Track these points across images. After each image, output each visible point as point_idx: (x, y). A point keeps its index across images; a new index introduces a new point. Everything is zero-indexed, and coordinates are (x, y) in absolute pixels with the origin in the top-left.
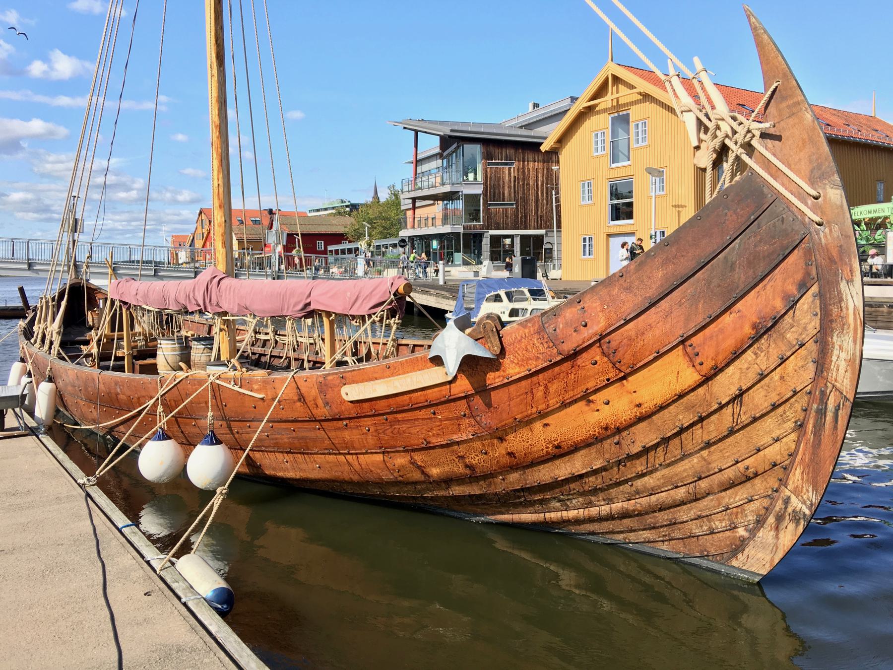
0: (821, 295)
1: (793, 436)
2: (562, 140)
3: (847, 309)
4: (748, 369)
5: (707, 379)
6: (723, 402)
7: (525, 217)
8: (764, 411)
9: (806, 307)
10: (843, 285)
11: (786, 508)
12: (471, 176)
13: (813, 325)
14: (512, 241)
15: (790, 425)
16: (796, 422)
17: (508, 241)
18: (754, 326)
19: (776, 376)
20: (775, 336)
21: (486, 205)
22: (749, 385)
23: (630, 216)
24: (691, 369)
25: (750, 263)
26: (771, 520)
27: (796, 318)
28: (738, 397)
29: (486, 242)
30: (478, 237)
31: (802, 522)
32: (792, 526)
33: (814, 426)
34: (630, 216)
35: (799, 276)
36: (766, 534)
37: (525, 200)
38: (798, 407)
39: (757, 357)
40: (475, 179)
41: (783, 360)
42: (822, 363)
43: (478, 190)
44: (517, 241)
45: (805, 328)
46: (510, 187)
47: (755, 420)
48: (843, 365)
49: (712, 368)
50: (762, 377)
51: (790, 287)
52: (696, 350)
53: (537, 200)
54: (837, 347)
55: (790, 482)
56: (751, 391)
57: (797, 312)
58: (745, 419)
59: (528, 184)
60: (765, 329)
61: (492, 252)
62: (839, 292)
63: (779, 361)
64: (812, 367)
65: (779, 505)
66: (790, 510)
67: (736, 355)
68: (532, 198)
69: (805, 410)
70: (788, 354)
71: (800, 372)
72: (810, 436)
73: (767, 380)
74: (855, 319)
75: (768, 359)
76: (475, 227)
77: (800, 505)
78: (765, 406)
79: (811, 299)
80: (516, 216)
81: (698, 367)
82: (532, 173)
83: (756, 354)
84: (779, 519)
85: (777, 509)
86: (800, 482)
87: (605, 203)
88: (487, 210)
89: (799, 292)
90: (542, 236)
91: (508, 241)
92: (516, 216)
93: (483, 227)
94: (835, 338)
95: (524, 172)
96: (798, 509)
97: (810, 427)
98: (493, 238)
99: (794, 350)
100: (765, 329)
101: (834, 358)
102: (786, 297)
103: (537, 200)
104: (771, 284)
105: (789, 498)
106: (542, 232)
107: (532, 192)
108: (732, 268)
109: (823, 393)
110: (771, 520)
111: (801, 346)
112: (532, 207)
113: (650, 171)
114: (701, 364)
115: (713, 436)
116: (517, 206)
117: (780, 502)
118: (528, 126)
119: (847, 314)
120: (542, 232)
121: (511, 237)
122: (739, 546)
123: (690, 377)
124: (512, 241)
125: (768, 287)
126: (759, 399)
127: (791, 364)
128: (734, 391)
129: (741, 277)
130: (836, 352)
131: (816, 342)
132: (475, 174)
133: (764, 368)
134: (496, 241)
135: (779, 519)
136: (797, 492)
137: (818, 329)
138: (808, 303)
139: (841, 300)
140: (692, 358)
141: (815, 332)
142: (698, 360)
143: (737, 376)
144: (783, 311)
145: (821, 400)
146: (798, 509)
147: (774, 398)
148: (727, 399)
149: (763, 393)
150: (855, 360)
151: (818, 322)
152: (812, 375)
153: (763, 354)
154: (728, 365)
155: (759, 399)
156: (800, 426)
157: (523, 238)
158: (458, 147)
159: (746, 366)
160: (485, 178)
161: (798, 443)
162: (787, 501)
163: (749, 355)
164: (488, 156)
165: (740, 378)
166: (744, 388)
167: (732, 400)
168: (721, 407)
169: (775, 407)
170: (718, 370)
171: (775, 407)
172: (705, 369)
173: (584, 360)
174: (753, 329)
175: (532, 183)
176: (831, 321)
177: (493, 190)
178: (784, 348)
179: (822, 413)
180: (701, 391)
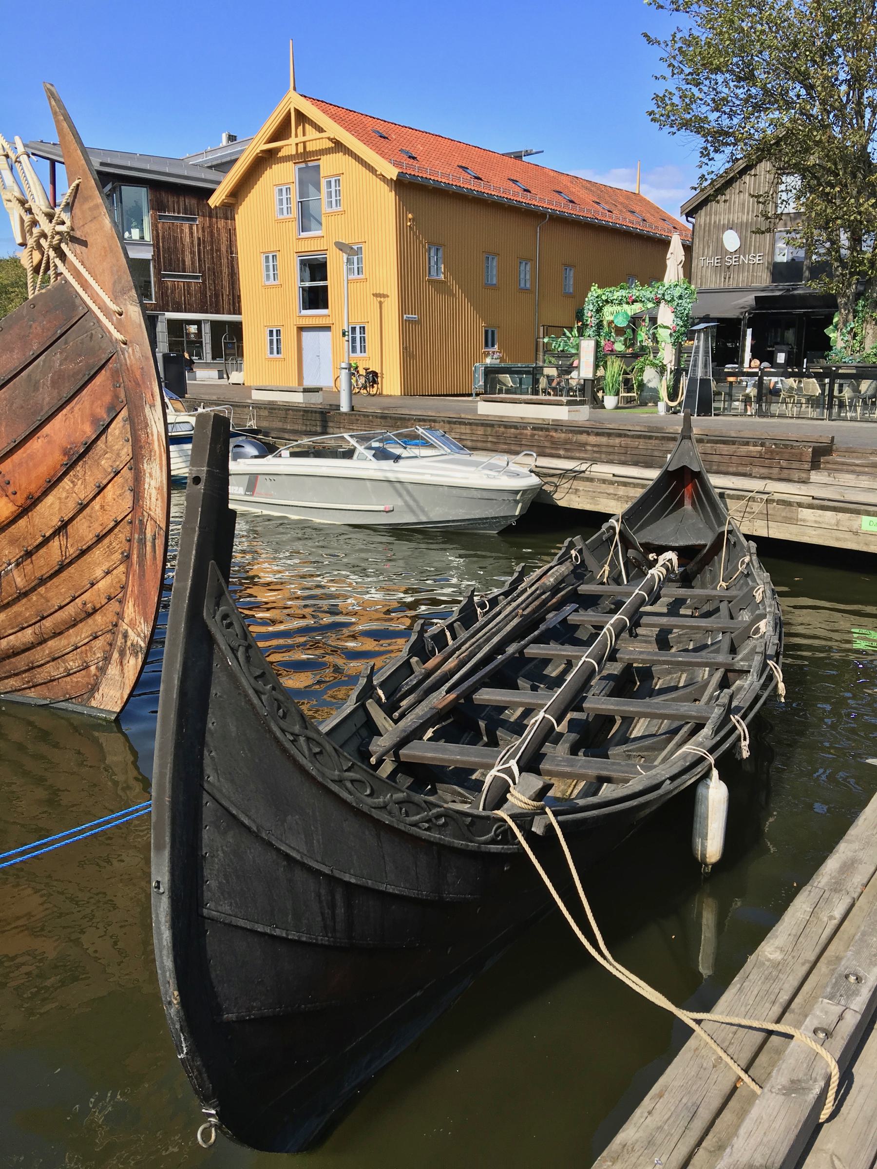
1: (122, 568)
3: (152, 435)
4: (67, 498)
5: (24, 511)
6: (47, 535)
8: (90, 543)
9: (117, 432)
10: (147, 409)
11: (126, 642)
13: (126, 451)
15: (117, 556)
16: (122, 553)
18: (66, 452)
19: (96, 504)
20: (89, 462)
22: (70, 515)
24: (5, 499)
25: (54, 383)
26: (116, 655)
27: (109, 444)
28: (63, 528)
31: (140, 654)
32: (132, 661)
33: (138, 557)
35: (107, 399)
36: (113, 670)
38: (122, 537)
39: (74, 486)
41: (101, 489)
42: (137, 491)
45: (118, 455)
47: (83, 553)
48: (154, 492)
49: (28, 498)
50: (83, 507)
51: (99, 410)
52: (7, 478)
54: (147, 475)
55: (126, 616)
56: (75, 522)
57: (110, 438)
58: (72, 551)
60: (77, 457)
62: (145, 416)
63: (97, 490)
64: (129, 496)
65: (120, 640)
66: (129, 643)
67: (52, 484)
69: (129, 541)
70: (105, 482)
72: (136, 567)
73: (88, 510)
74: (159, 445)
75: (85, 487)
77: (136, 638)
78: (90, 538)
79: (121, 424)
81: (12, 497)
83: (73, 482)
84: (122, 653)
85: (119, 643)
86: (133, 614)
89: (108, 415)
94: (145, 465)
96: (135, 642)
97: (135, 557)
99: (109, 478)
100: (77, 457)
101: (146, 486)
102: (95, 421)
104: (78, 406)
105: (127, 631)
108: (36, 388)
109: (141, 521)
110: (116, 655)
111: (117, 473)
114: (15, 493)
115: (45, 571)
117: (120, 636)
119: (153, 440)
122: (94, 688)
125: (76, 409)
126: (84, 530)
127: (109, 491)
128: (56, 522)
129: (46, 398)
130: (147, 480)
131: (131, 469)
133: (82, 497)
135: (122, 653)
136: (132, 624)
137: (131, 456)
138: (118, 428)
139: (147, 425)
141: (128, 458)
142: (11, 489)
143: (57, 506)
144: (94, 437)
145: (141, 529)
146: (135, 642)
147: (98, 529)
148: (50, 532)
149: (86, 524)
150: (162, 487)
151: (130, 447)
152: (130, 504)
153: (80, 482)
154: (45, 493)
155: (84, 530)
156: (127, 558)
159: (64, 495)
161: (127, 574)
162: (125, 636)
163: (66, 483)
165: (60, 509)
166: (66, 519)
167: (57, 532)
168: (46, 541)
169: (100, 539)
171: (100, 539)
172: (20, 499)
174: (65, 455)
176: (141, 447)
178: (99, 476)
179: (142, 542)
180: (22, 522)
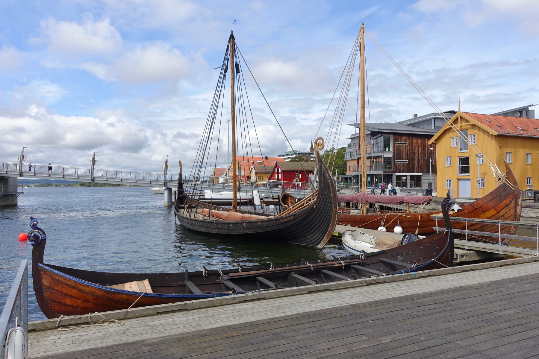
0: (515, 201)
2: (437, 140)
5: (498, 213)
7: (413, 167)
12: (387, 149)
13: (514, 205)
14: (406, 178)
17: (404, 178)
21: (394, 161)
23: (468, 172)
29: (394, 178)
30: (391, 176)
34: (468, 172)
37: (413, 160)
40: (389, 150)
43: (391, 155)
44: (409, 178)
46: (405, 154)
53: (418, 160)
59: (414, 152)
60: (507, 205)
61: (397, 183)
67: (502, 209)
68: (416, 159)
71: (512, 212)
76: (389, 172)
80: (408, 167)
82: (416, 147)
87: (457, 166)
88: (395, 164)
90: (421, 176)
91: (404, 178)
92: (408, 167)
93: (392, 172)
95: (412, 148)
98: (397, 176)
100: (507, 205)
103: (418, 160)
106: (421, 174)
107: (416, 156)
112: (416, 162)
113: (477, 156)
116: (409, 162)
118: (412, 125)
120: (421, 174)
121: (406, 176)
123: (495, 212)
124: (406, 178)
132: (389, 148)
134: (399, 178)
138: (513, 202)
140: (495, 210)
157: (411, 176)
158: (381, 136)
160: (394, 150)
164: (395, 140)
170: (500, 211)
173: (478, 210)
175: (416, 152)
177: (397, 155)
